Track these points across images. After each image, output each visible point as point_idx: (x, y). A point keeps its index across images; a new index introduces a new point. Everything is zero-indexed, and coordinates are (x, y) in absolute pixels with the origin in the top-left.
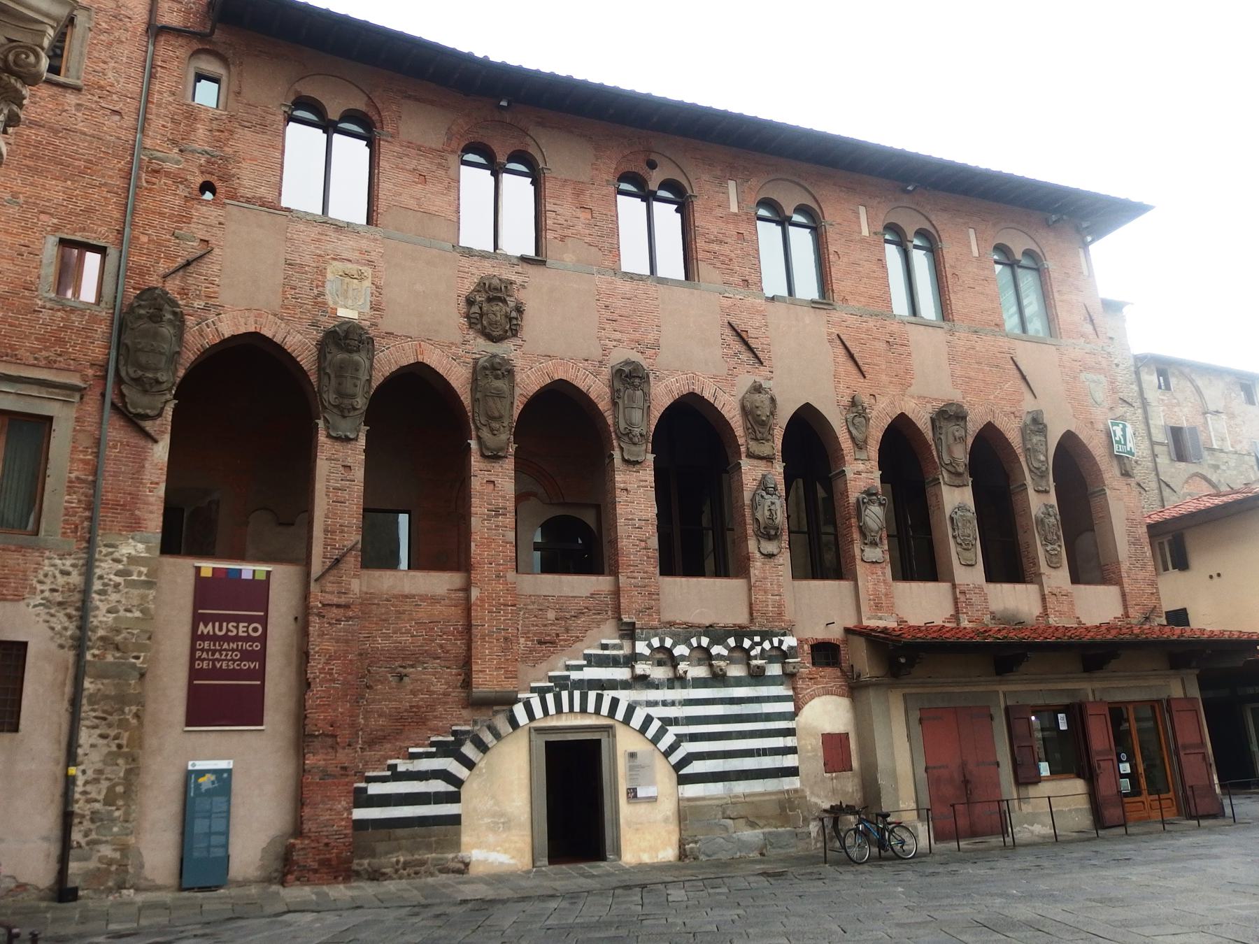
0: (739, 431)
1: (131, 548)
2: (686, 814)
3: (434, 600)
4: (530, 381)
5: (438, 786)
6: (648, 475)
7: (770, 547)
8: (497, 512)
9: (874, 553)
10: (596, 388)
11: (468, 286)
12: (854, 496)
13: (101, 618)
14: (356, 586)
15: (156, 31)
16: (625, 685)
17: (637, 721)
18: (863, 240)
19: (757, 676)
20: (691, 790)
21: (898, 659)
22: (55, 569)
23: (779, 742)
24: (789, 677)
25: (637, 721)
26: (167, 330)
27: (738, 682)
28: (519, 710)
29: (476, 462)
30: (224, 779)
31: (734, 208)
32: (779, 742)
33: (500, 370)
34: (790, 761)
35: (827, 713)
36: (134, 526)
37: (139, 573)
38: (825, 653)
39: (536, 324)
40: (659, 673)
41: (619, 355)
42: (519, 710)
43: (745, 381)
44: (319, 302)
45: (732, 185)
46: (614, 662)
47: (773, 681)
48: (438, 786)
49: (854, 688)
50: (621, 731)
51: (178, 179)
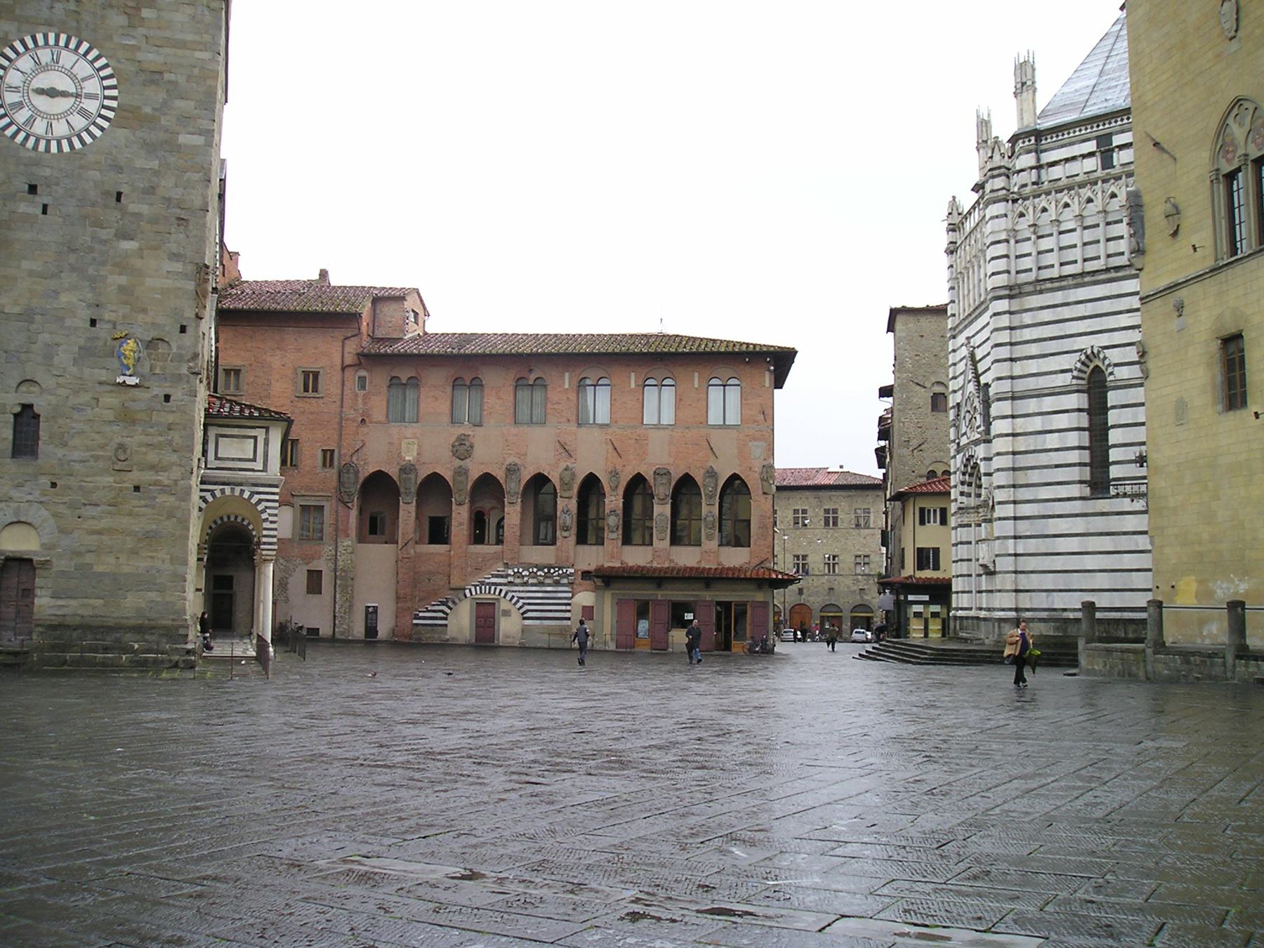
0: (558, 488)
1: (347, 542)
2: (524, 630)
3: (440, 554)
4: (475, 474)
5: (441, 615)
6: (518, 507)
7: (565, 534)
8: (461, 524)
9: (614, 536)
10: (500, 474)
11: (453, 439)
12: (607, 511)
13: (340, 563)
14: (412, 552)
15: (343, 369)
16: (505, 585)
17: (508, 597)
18: (631, 390)
19: (557, 583)
20: (527, 622)
21: (605, 579)
22: (328, 549)
23: (563, 608)
24: (571, 584)
25: (508, 597)
26: (352, 476)
27: (549, 585)
28: (467, 592)
29: (454, 507)
30: (375, 608)
31: (567, 386)
32: (563, 608)
33: (461, 472)
34: (567, 615)
35: (585, 598)
36: (348, 536)
37: (350, 550)
38: (586, 575)
39: (479, 452)
40: (518, 581)
41: (511, 460)
42: (467, 592)
43: (563, 465)
44: (399, 455)
45: (567, 375)
46: (502, 576)
47: (564, 585)
48: (441, 615)
49: (596, 589)
50: (502, 601)
51: (354, 420)
